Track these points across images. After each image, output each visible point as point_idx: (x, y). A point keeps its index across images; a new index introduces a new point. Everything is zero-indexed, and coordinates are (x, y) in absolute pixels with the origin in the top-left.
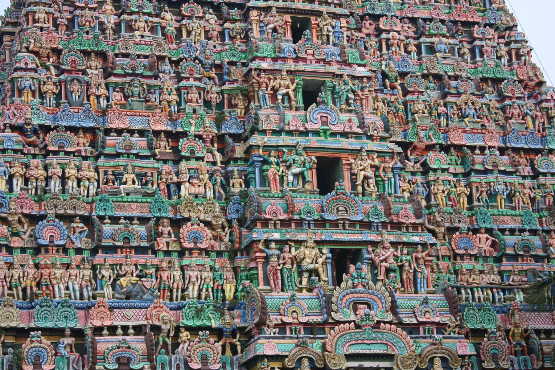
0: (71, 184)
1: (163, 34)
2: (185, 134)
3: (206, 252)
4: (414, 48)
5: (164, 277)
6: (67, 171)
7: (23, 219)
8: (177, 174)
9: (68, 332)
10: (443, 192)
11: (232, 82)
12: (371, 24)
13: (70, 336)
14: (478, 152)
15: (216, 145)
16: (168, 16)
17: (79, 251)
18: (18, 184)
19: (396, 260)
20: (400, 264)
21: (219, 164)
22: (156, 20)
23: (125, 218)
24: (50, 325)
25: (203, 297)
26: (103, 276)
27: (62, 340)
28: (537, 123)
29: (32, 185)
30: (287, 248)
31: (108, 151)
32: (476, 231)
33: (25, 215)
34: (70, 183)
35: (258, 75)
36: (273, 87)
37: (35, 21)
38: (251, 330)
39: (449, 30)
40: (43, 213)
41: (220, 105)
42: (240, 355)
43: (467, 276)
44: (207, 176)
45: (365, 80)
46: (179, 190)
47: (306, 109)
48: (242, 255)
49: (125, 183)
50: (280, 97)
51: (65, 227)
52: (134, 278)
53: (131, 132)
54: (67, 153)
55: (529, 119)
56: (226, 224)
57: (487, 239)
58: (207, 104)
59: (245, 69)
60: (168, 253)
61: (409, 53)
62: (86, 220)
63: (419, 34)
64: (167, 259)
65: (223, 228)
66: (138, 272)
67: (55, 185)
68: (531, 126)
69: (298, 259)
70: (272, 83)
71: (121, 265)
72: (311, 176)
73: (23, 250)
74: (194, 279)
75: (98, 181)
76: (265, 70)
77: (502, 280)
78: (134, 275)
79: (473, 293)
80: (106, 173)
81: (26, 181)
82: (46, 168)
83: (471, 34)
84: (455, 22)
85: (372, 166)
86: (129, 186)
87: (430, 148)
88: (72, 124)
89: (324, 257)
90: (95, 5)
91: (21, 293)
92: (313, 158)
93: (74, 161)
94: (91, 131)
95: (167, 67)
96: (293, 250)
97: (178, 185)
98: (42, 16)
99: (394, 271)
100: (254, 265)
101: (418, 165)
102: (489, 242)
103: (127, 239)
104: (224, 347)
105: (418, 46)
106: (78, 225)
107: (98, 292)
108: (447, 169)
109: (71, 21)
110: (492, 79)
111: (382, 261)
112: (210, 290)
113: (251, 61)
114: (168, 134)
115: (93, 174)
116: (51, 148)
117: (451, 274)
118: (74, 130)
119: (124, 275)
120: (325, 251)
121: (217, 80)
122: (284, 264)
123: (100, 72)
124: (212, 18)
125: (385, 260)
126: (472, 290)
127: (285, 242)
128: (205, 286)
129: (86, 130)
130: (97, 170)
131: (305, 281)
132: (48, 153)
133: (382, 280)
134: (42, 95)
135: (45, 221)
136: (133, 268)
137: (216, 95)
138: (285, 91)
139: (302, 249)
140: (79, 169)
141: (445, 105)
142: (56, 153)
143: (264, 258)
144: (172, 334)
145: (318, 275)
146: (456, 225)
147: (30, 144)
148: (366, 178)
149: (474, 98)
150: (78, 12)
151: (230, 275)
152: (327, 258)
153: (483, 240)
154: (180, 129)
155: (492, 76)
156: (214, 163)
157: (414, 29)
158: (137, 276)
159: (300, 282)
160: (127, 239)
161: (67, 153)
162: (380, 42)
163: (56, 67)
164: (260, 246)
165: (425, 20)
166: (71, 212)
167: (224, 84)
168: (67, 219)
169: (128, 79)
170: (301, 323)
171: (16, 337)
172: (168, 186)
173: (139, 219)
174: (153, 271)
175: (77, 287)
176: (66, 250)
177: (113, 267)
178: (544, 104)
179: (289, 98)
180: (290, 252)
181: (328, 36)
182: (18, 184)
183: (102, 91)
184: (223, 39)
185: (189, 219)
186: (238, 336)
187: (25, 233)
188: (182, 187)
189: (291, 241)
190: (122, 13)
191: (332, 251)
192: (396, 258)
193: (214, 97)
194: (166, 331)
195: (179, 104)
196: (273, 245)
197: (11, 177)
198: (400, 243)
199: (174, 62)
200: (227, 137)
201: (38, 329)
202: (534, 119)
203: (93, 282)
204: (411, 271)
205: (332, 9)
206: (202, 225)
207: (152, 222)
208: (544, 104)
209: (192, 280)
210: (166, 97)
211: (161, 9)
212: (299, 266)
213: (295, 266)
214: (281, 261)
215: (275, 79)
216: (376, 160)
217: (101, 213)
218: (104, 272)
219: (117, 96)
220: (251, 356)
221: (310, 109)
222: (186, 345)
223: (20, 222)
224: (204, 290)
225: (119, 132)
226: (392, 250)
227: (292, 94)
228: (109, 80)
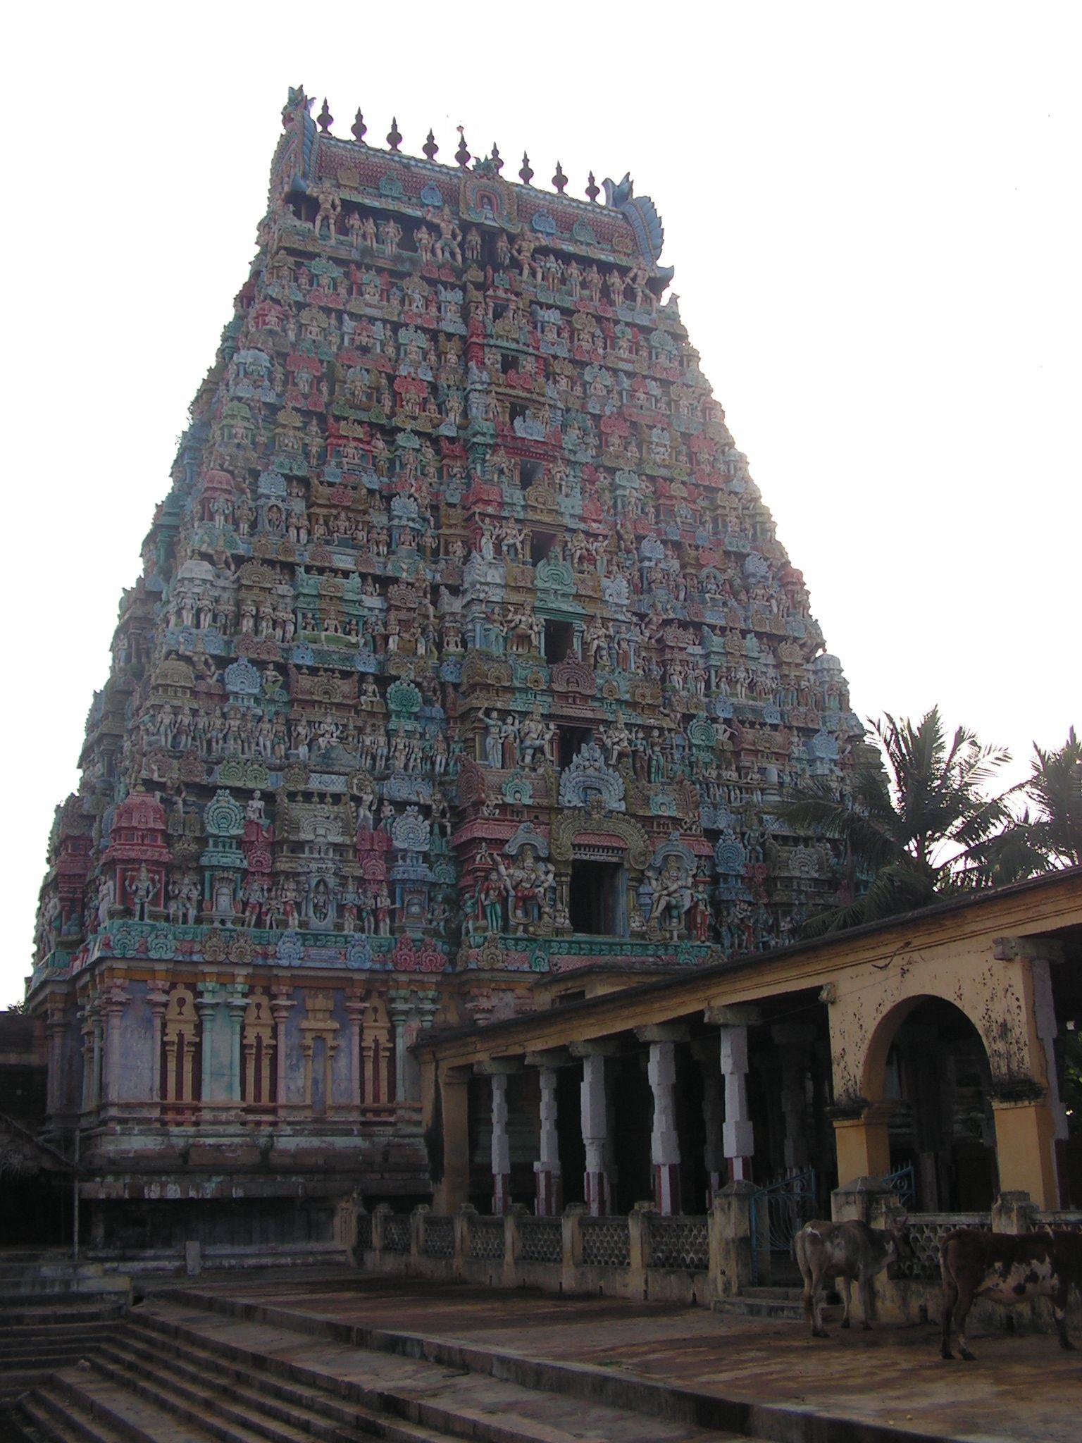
2: (396, 580)
3: (416, 717)
4: (652, 510)
5: (368, 743)
6: (262, 609)
7: (210, 661)
8: (385, 625)
9: (258, 794)
10: (680, 673)
11: (450, 526)
12: (605, 478)
13: (260, 799)
14: (718, 632)
15: (429, 596)
16: (381, 444)
18: (206, 620)
19: (630, 745)
20: (633, 748)
21: (432, 618)
22: (367, 447)
23: (326, 670)
24: (239, 784)
25: (411, 767)
26: (299, 734)
27: (250, 802)
28: (781, 607)
30: (510, 720)
32: (714, 720)
33: (213, 657)
34: (264, 624)
35: (483, 521)
36: (499, 536)
38: (465, 810)
39: (690, 494)
40: (233, 655)
42: (449, 838)
43: (704, 771)
44: (420, 630)
45: (601, 538)
46: (387, 644)
47: (534, 565)
48: (455, 723)
49: (326, 630)
50: (505, 548)
51: (258, 674)
52: (334, 739)
55: (773, 601)
56: (437, 687)
57: (725, 731)
59: (467, 514)
60: (371, 714)
61: (647, 514)
62: (282, 668)
63: (657, 494)
64: (370, 721)
65: (434, 691)
66: (339, 732)
67: (248, 624)
68: (775, 610)
69: (522, 734)
70: (497, 531)
71: (320, 723)
72: (539, 641)
73: (209, 695)
74: (401, 747)
75: (295, 624)
76: (490, 516)
77: (740, 777)
78: (335, 735)
79: (708, 789)
80: (304, 616)
83: (712, 500)
84: (697, 486)
85: (606, 636)
86: (331, 633)
87: (667, 623)
89: (551, 733)
90: (301, 425)
91: (205, 745)
92: (542, 620)
96: (517, 722)
97: (386, 638)
98: (241, 431)
99: (627, 756)
100: (471, 736)
101: (653, 641)
102: (728, 734)
104: (431, 826)
105: (657, 508)
106: (271, 673)
107: (292, 751)
108: (685, 649)
110: (735, 553)
111: (614, 744)
112: (419, 761)
113: (475, 503)
116: (244, 582)
117: (685, 766)
119: (323, 735)
120: (552, 726)
121: (432, 523)
122: (506, 737)
125: (617, 743)
126: (707, 785)
127: (509, 712)
128: (413, 756)
131: (528, 759)
133: (614, 766)
135: (235, 665)
136: (333, 727)
137: (431, 540)
138: (512, 541)
139: (527, 722)
141: (684, 577)
143: (483, 728)
144: (374, 808)
145: (543, 753)
146: (693, 711)
148: (599, 647)
149: (716, 571)
150: (279, 430)
151: (442, 746)
152: (555, 734)
153: (721, 731)
154: (390, 574)
155: (735, 549)
156: (427, 617)
157: (653, 489)
158: (337, 737)
159: (523, 760)
162: (615, 499)
163: (252, 491)
164: (480, 714)
165: (665, 479)
166: (264, 657)
167: (440, 528)
169: (334, 512)
170: (525, 805)
171: (199, 796)
172: (374, 637)
173: (341, 672)
175: (268, 744)
177: (310, 723)
178: (790, 587)
179: (516, 550)
180: (513, 724)
181: (561, 485)
182: (206, 620)
185: (397, 678)
186: (448, 815)
187: (211, 677)
188: (391, 640)
189: (514, 711)
190: (328, 437)
191: (559, 727)
192: (630, 741)
194: (368, 803)
196: (495, 714)
197: (199, 611)
198: (635, 725)
199: (384, 497)
200: (443, 588)
201: (226, 788)
202: (779, 603)
203: (286, 739)
204: (646, 758)
206: (412, 685)
207: (356, 677)
208: (790, 587)
209: (399, 747)
210: (375, 536)
211: (372, 436)
212: (522, 742)
213: (518, 741)
214: (503, 735)
215: (501, 527)
216: (611, 629)
217: (300, 662)
218: (300, 729)
220: (464, 839)
221: (540, 565)
222: (390, 821)
223: (206, 662)
224: (412, 760)
226: (627, 732)
227: (519, 546)
228: (312, 510)
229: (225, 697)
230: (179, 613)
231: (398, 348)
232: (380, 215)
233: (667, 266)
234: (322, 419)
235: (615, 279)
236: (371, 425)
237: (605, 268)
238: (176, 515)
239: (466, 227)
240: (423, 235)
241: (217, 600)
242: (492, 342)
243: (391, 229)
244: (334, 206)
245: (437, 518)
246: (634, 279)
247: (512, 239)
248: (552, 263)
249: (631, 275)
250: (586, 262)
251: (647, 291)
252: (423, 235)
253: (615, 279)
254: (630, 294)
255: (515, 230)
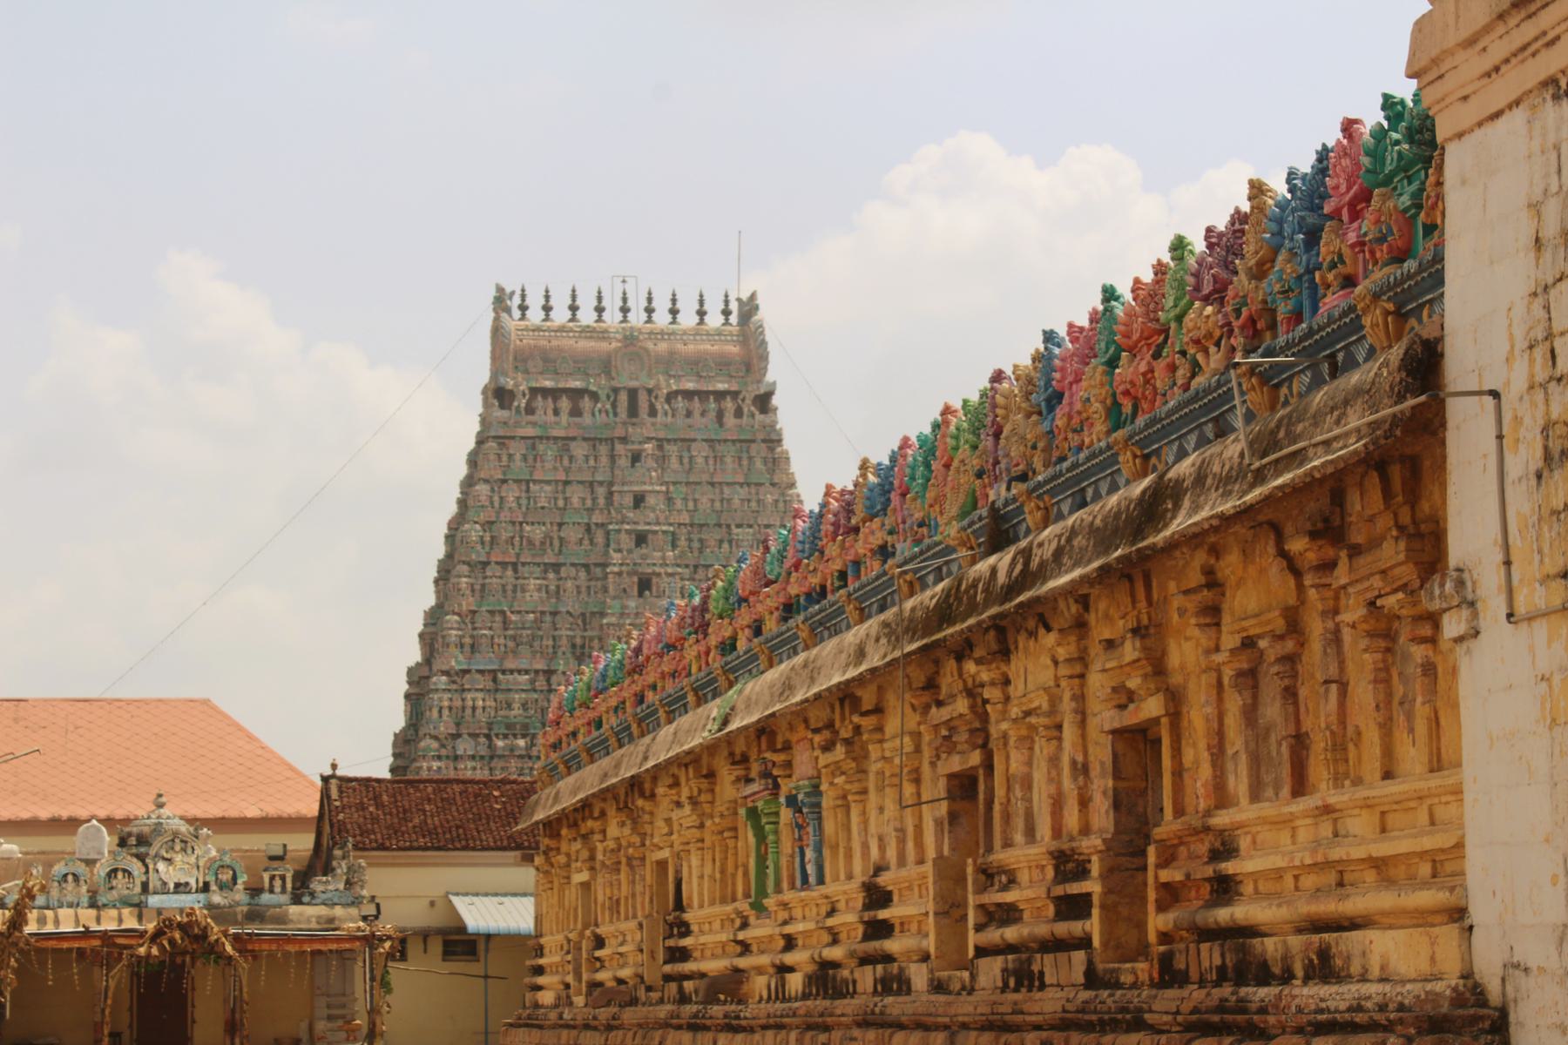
0: (478, 712)
1: (547, 592)
11: (592, 629)
16: (551, 575)
17: (482, 757)
18: (446, 712)
29: (454, 711)
31: (503, 686)
37: (459, 590)
41: (583, 647)
53: (519, 672)
54: (477, 690)
58: (574, 646)
67: (468, 712)
73: (448, 757)
81: (450, 708)
82: (463, 700)
88: (481, 667)
93: (480, 695)
94: (494, 672)
95: (548, 618)
103: (512, 750)
106: (482, 740)
109: (483, 586)
114: (545, 672)
115: (493, 704)
116: (466, 687)
118: (481, 672)
123: (501, 625)
124: (583, 574)
129: (490, 671)
130: (495, 700)
132: (464, 690)
134: (462, 646)
140: (484, 700)
142: (469, 690)
147: (454, 682)
160: (512, 750)
161: (477, 690)
168: (474, 736)
174: (527, 771)
176: (473, 757)
182: (446, 712)
183: (502, 641)
184: (589, 594)
193: (578, 641)
195: (554, 647)
205: (670, 570)
219: (511, 644)
225: (512, 672)
229: (456, 758)
230: (430, 710)
231: (566, 499)
232: (554, 393)
233: (771, 381)
234: (514, 565)
235: (729, 404)
236: (545, 564)
237: (720, 395)
238: (434, 624)
239: (616, 391)
240: (586, 403)
241: (451, 700)
242: (626, 488)
243: (565, 403)
244: (524, 395)
245: (585, 624)
246: (743, 400)
247: (650, 391)
248: (680, 403)
249: (741, 397)
250: (702, 395)
251: (753, 408)
252: (586, 403)
253: (729, 404)
254: (739, 413)
255: (651, 384)
